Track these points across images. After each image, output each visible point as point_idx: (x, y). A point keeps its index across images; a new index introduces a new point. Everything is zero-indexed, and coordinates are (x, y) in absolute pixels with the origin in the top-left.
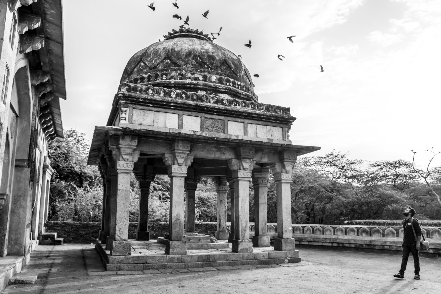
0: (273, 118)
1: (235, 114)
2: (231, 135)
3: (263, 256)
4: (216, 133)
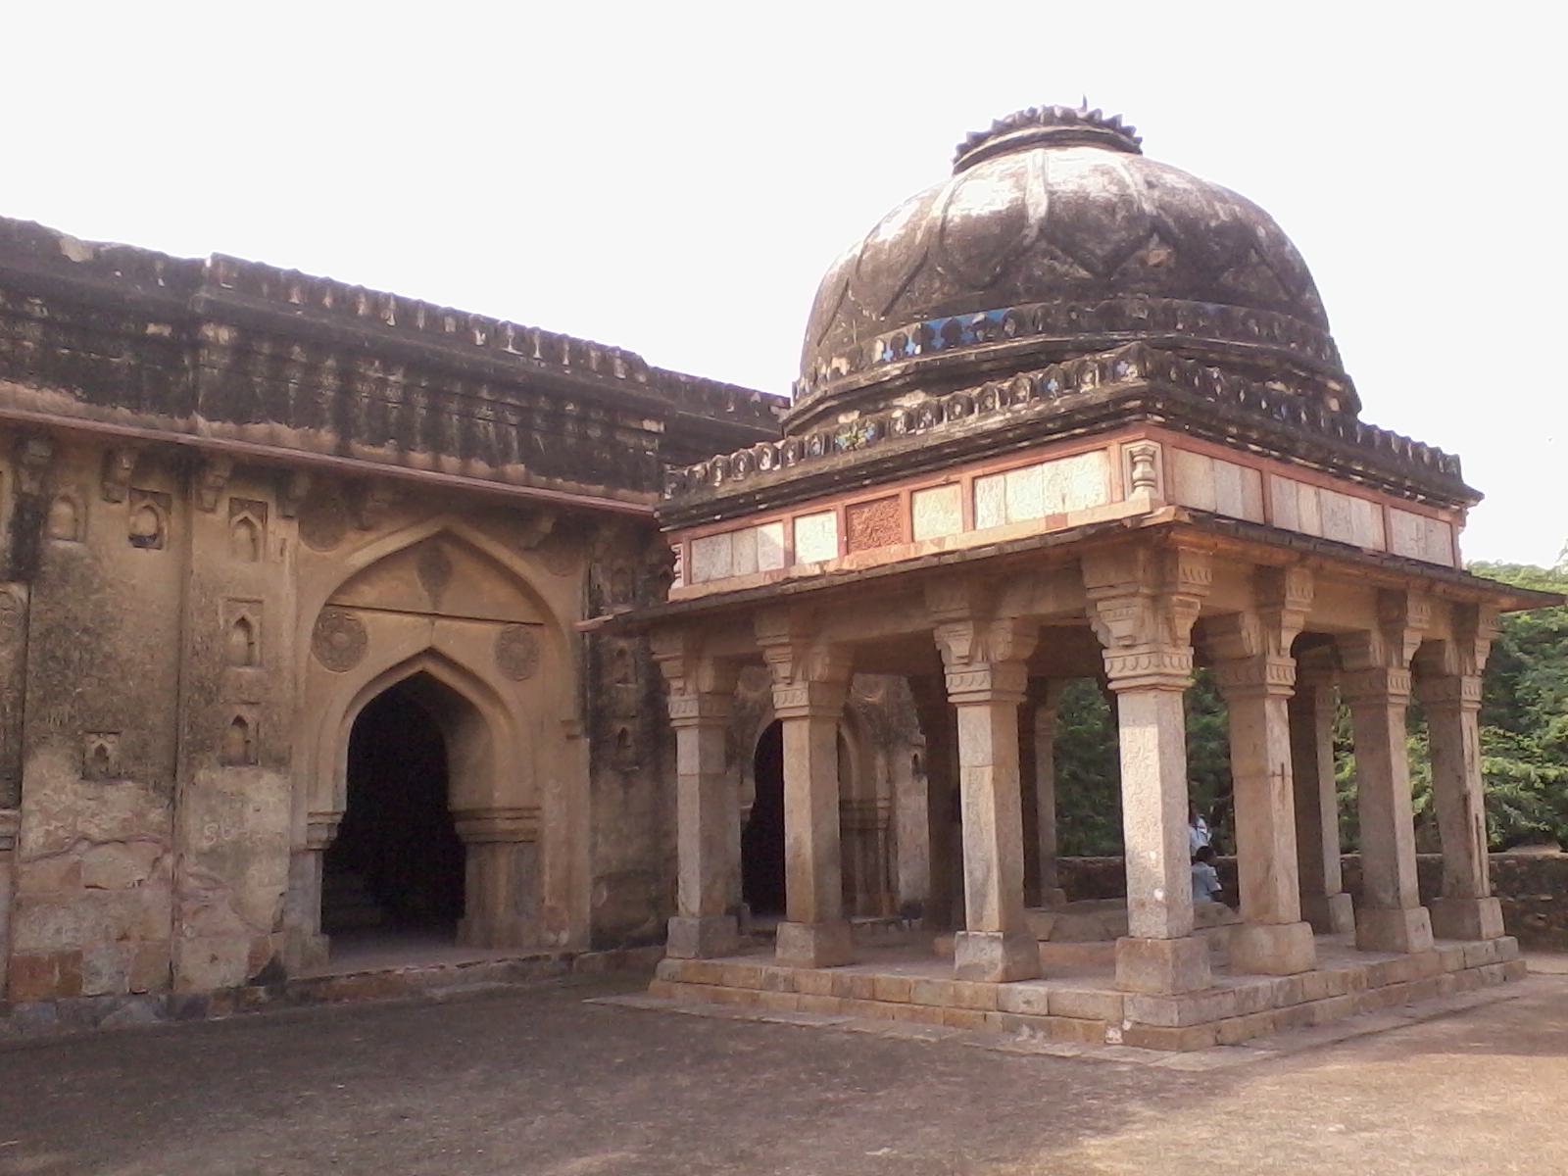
0: (1050, 426)
1: (954, 455)
2: (922, 543)
3: (1028, 1002)
4: (877, 551)
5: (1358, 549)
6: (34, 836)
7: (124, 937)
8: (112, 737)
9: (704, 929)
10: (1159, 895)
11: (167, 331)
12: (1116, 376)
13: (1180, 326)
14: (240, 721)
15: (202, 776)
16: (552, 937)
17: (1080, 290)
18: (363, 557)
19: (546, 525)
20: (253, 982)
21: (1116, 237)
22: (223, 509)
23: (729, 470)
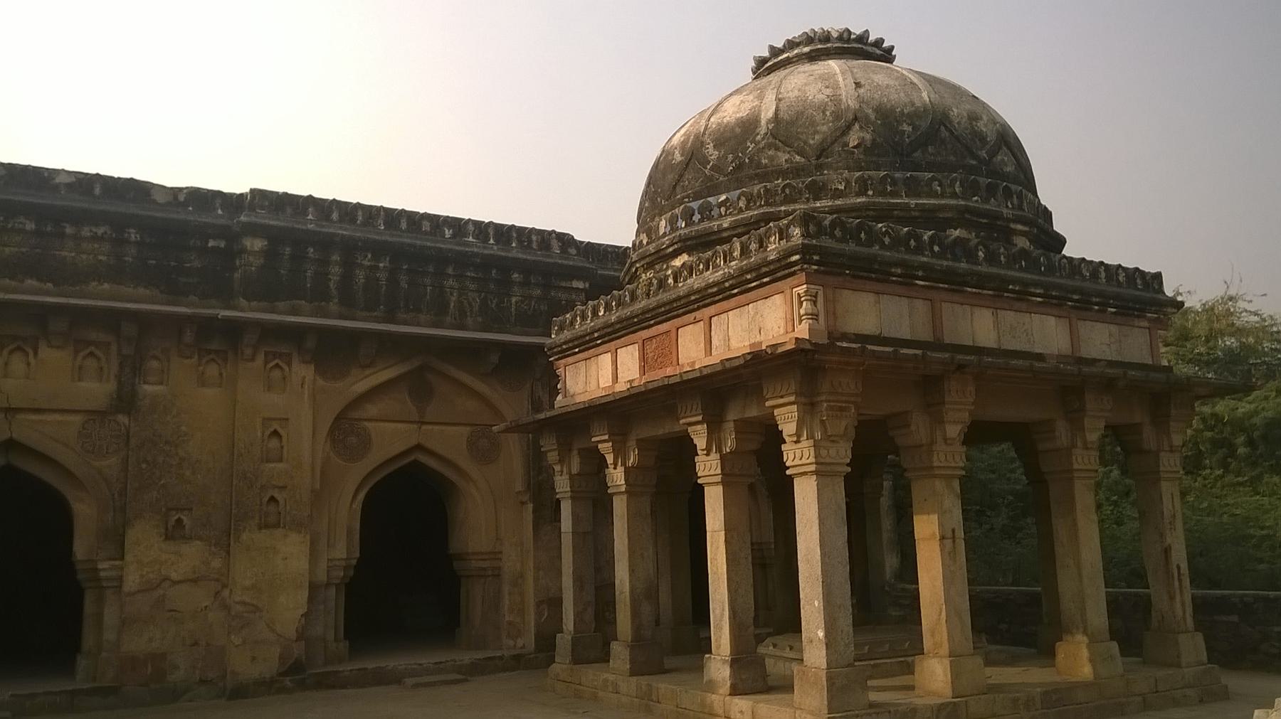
0: (749, 277)
5: (1040, 357)
6: (132, 580)
7: (196, 644)
8: (186, 512)
9: (575, 642)
10: (821, 634)
11: (222, 244)
12: (788, 238)
13: (870, 193)
14: (272, 499)
15: (245, 536)
16: (511, 643)
17: (797, 171)
18: (362, 386)
19: (494, 358)
20: (280, 674)
21: (825, 128)
22: (260, 358)
23: (584, 318)
